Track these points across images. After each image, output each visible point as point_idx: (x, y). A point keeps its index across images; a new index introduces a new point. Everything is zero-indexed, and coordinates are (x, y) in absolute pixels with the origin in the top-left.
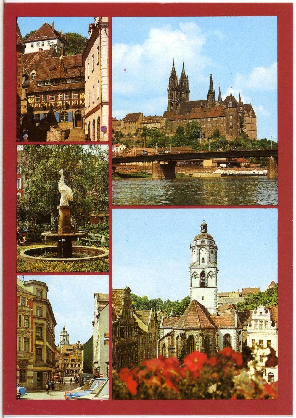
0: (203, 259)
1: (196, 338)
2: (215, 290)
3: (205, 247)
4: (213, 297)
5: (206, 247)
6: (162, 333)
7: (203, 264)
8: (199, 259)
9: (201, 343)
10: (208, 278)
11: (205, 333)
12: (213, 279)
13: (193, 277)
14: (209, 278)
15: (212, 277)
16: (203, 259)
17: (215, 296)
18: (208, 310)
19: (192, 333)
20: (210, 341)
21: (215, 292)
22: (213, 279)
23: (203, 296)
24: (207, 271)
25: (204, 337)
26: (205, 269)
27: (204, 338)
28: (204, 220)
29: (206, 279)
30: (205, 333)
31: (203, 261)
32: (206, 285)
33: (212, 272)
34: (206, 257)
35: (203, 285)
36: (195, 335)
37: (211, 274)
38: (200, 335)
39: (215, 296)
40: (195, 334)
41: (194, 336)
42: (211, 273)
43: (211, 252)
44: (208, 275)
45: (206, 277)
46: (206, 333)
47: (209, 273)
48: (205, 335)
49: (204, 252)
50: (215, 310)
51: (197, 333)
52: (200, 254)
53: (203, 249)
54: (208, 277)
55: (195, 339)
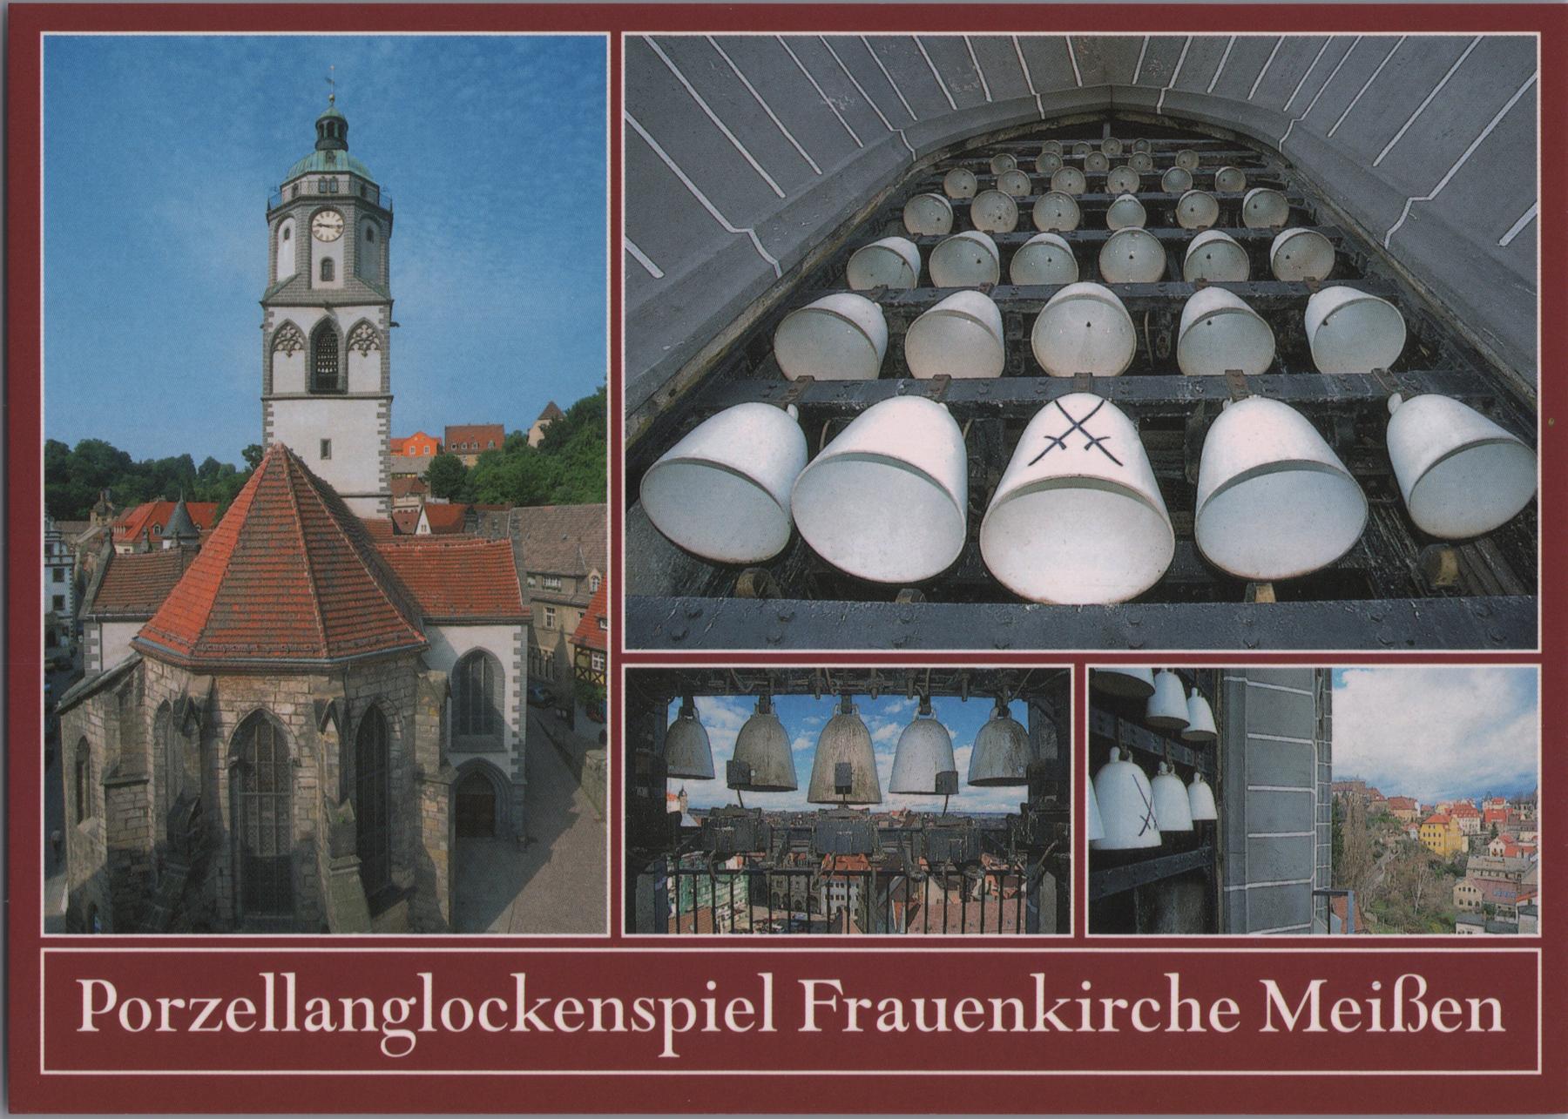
0: (327, 263)
2: (383, 410)
4: (375, 445)
5: (343, 209)
6: (95, 650)
7: (327, 285)
8: (310, 265)
9: (336, 781)
10: (351, 354)
12: (375, 357)
14: (355, 356)
15: (368, 348)
16: (327, 263)
17: (383, 437)
18: (348, 501)
21: (383, 421)
22: (375, 357)
23: (326, 437)
24: (346, 319)
26: (337, 310)
29: (341, 354)
31: (327, 275)
32: (339, 387)
33: (370, 325)
34: (339, 253)
35: (326, 383)
36: (289, 709)
39: (383, 437)
40: (288, 703)
42: (364, 332)
43: (364, 234)
44: (350, 337)
45: (341, 346)
47: (353, 331)
49: (332, 233)
50: (383, 507)
51: (302, 700)
52: (314, 240)
53: (331, 218)
54: (349, 349)
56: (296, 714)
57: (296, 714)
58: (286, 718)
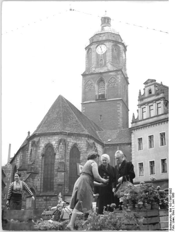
1: (55, 147)
3: (104, 44)
11: (70, 140)
13: (87, 87)
19: (50, 140)
20: (81, 155)
25: (70, 148)
27: (68, 149)
28: (106, 11)
30: (70, 140)
37: (113, 81)
38: (60, 141)
41: (52, 145)
46: (72, 141)
48: (71, 144)
51: (57, 140)
55: (55, 149)
56: (56, 143)
57: (56, 143)
58: (54, 145)
